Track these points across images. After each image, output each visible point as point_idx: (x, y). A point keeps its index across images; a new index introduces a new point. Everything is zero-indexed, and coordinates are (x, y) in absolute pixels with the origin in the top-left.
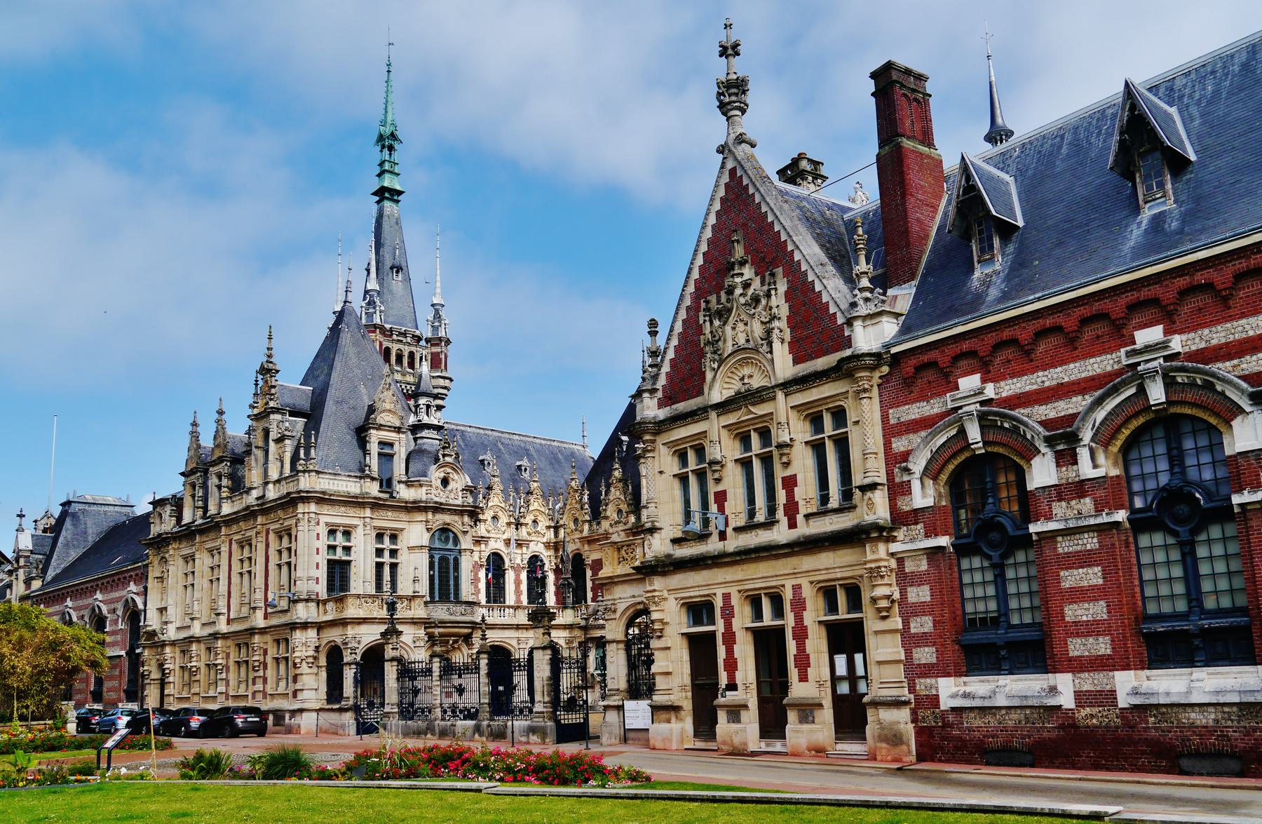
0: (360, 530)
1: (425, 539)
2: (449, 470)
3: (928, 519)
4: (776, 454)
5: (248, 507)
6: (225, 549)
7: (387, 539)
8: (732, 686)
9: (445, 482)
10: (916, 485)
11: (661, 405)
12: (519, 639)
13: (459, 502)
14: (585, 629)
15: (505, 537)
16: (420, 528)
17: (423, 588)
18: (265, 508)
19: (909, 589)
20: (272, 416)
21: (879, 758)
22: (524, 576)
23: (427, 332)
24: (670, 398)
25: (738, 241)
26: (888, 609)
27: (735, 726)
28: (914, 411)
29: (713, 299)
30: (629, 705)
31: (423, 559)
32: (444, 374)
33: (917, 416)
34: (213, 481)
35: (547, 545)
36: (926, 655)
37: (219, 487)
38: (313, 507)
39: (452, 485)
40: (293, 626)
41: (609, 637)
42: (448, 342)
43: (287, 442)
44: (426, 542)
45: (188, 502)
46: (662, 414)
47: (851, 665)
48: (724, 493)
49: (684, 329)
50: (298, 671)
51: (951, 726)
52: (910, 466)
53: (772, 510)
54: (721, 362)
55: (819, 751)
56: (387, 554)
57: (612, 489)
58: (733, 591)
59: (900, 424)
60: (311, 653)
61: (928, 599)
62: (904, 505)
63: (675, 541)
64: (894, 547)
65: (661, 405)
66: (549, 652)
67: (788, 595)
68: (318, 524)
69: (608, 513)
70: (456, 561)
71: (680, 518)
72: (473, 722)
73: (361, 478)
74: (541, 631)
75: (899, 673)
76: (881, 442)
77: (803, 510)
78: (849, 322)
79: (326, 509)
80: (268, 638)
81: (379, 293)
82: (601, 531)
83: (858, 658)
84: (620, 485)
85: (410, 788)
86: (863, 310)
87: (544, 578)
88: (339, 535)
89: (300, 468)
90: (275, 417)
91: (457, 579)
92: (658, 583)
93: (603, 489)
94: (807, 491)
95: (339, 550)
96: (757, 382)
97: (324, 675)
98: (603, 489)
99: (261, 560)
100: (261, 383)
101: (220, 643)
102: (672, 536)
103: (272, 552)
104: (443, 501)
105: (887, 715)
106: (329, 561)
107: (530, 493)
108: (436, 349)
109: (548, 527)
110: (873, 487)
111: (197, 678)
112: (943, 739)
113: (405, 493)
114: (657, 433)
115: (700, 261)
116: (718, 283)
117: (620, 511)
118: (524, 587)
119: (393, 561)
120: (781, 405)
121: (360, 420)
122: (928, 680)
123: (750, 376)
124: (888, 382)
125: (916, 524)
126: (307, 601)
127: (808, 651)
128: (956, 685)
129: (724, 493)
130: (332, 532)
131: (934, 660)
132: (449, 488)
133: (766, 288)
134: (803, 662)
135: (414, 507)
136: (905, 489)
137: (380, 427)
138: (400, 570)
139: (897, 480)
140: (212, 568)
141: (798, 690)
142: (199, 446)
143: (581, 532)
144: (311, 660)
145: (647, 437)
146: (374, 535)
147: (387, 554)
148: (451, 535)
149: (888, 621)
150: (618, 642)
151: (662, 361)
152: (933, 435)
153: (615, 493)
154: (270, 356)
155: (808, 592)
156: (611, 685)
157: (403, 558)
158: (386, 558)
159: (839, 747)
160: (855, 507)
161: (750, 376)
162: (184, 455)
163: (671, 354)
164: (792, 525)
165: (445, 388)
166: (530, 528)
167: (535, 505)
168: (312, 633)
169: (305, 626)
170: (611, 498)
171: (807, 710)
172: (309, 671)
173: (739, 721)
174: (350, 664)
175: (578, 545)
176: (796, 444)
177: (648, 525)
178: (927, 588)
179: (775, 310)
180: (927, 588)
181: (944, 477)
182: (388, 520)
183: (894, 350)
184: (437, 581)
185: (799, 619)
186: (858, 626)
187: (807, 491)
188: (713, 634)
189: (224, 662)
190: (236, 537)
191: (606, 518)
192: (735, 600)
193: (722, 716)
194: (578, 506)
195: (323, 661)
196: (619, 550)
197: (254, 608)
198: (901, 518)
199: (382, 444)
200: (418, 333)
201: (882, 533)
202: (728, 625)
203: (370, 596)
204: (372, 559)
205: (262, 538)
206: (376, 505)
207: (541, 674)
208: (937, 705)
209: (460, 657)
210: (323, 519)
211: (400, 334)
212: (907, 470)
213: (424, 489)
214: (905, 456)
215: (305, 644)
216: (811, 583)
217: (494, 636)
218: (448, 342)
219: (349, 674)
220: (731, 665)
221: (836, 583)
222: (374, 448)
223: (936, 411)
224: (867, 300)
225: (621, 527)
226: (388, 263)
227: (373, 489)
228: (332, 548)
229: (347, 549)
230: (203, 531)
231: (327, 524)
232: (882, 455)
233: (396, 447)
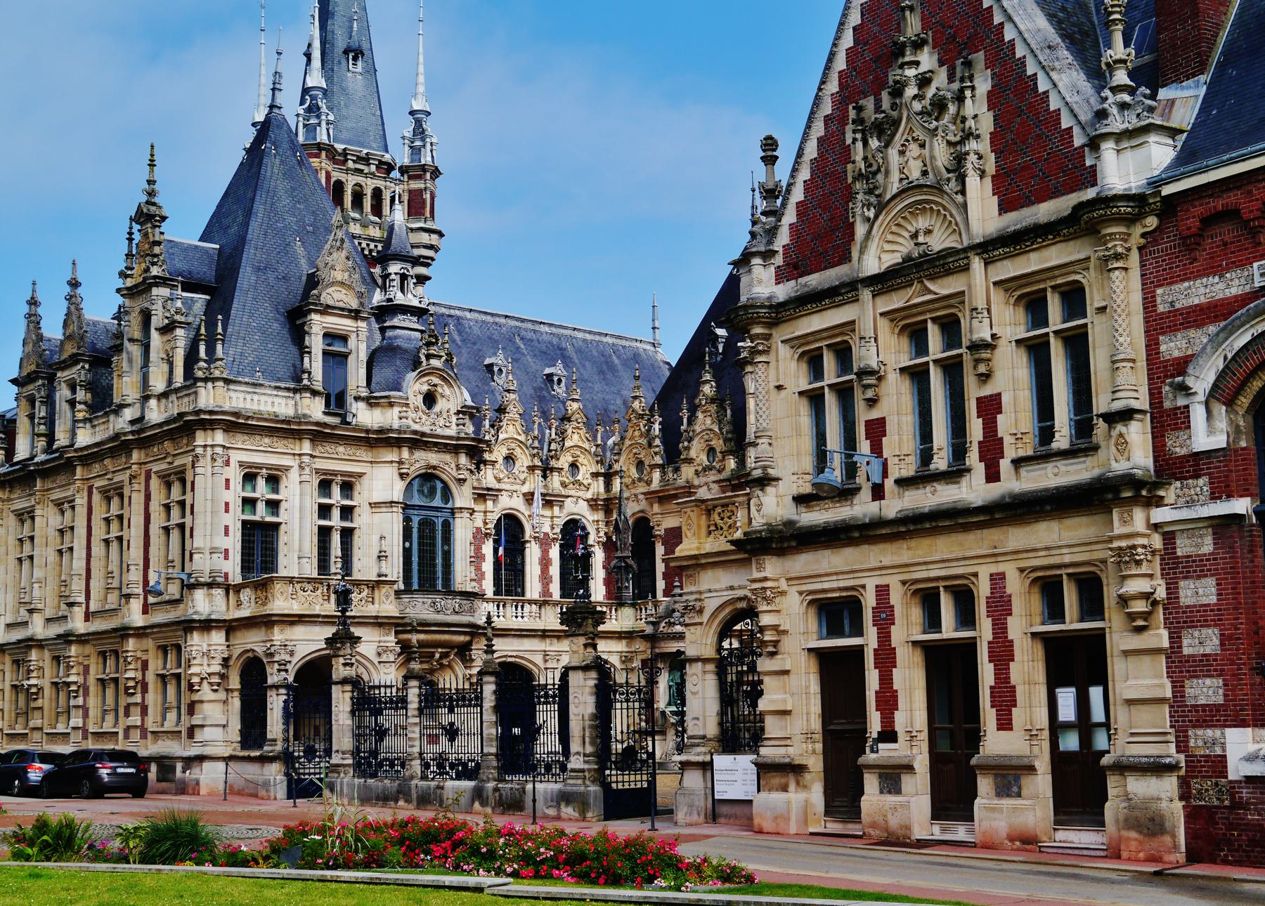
0: (294, 475)
1: (397, 490)
2: (436, 380)
3: (1219, 471)
4: (967, 359)
5: (117, 436)
6: (81, 501)
7: (336, 490)
8: (888, 735)
9: (430, 399)
10: (1198, 414)
11: (781, 277)
12: (545, 654)
13: (452, 432)
14: (653, 639)
15: (525, 489)
16: (390, 473)
17: (394, 569)
18: (145, 437)
19: (1182, 583)
20: (155, 291)
21: (1125, 854)
22: (555, 552)
23: (402, 157)
24: (796, 267)
25: (911, 9)
26: (1146, 616)
27: (891, 799)
28: (1198, 292)
29: (869, 103)
30: (721, 761)
31: (393, 523)
32: (429, 225)
33: (1203, 300)
34: (63, 393)
35: (593, 504)
36: (1206, 691)
37: (72, 403)
38: (219, 437)
39: (441, 405)
40: (189, 626)
41: (691, 652)
42: (436, 173)
43: (180, 332)
44: (398, 495)
45: (23, 426)
46: (782, 292)
47: (1083, 704)
48: (881, 422)
49: (820, 154)
50: (196, 697)
51: (1245, 806)
52: (1190, 382)
53: (959, 451)
54: (881, 207)
55: (1027, 841)
56: (336, 513)
57: (700, 415)
58: (894, 581)
59: (1174, 313)
60: (216, 668)
61: (1213, 599)
62: (1177, 447)
63: (802, 500)
64: (1160, 515)
65: (781, 277)
66: (594, 674)
67: (983, 589)
68: (227, 463)
69: (693, 454)
70: (447, 527)
71: (808, 463)
72: (472, 784)
73: (295, 391)
74: (582, 640)
75: (1161, 719)
76: (1141, 342)
77: (1010, 452)
78: (1094, 144)
79: (240, 440)
80: (149, 643)
81: (325, 92)
82: (681, 482)
83: (1096, 693)
84: (713, 408)
85: (371, 882)
86: (1117, 123)
87: (588, 555)
88: (261, 483)
89: (200, 374)
90: (161, 292)
91: (447, 556)
92: (772, 568)
93: (685, 414)
94: (1016, 420)
95: (261, 507)
96: (939, 241)
97: (236, 703)
98: (685, 414)
99: (137, 520)
100: (137, 237)
101: (74, 650)
102: (795, 492)
103: (155, 507)
104: (426, 429)
105: (1140, 787)
106: (245, 523)
107: (566, 419)
108: (416, 185)
109: (595, 475)
110: (1127, 415)
111: (39, 703)
112: (1231, 827)
113: (365, 417)
114: (774, 323)
115: (848, 40)
116: (876, 78)
117: (711, 451)
118: (555, 570)
119: (347, 524)
120: (979, 280)
121: (294, 301)
122: (1209, 732)
123: (928, 232)
124: (1155, 242)
125: (1197, 477)
126: (210, 586)
127: (1013, 682)
128: (1255, 741)
129: (881, 422)
130: (249, 478)
131: (1220, 700)
132: (437, 408)
133: (956, 86)
134: (1005, 698)
135: (380, 440)
136: (1180, 420)
137: (326, 310)
138: (358, 540)
139: (1167, 404)
140: (61, 532)
141: (996, 743)
142: (40, 338)
143: (649, 483)
144: (216, 679)
145: (757, 330)
146: (316, 483)
147: (336, 513)
148: (439, 485)
149: (1146, 635)
150: (705, 661)
151: (784, 205)
152: (1230, 331)
153: (704, 421)
154: (151, 194)
155: (1015, 585)
156: (692, 729)
157: (363, 520)
158: (335, 520)
159: (1060, 835)
160: (1096, 448)
161: (928, 232)
162: (17, 352)
163: (798, 195)
164: (993, 475)
165: (431, 247)
166: (568, 479)
167: (575, 438)
168: (218, 637)
169: (207, 625)
170: (698, 428)
171: (1010, 776)
172: (213, 696)
173: (898, 791)
174: (276, 687)
175: (643, 504)
176: (1002, 343)
177: (757, 473)
178: (1211, 582)
179: (970, 123)
180: (1211, 582)
181: (1244, 401)
182: (338, 460)
183: (1167, 190)
184: (415, 559)
185: (1000, 629)
186: (1098, 639)
187: (1016, 420)
188: (859, 651)
189: (80, 680)
190: (99, 483)
191: (689, 461)
192: (897, 597)
193: (871, 783)
194: (644, 441)
195: (235, 682)
196: (709, 512)
197: (128, 596)
198: (1172, 467)
199: (330, 336)
200: (387, 158)
201: (1141, 491)
202: (884, 637)
203: (310, 580)
204: (313, 522)
205: (139, 485)
206: (319, 435)
207: (581, 710)
208: (1223, 772)
209: (452, 679)
210: (236, 457)
211: (359, 159)
212: (1184, 389)
213: (396, 410)
214: (1182, 365)
215: (207, 654)
216: (1022, 570)
217: (505, 648)
218: (436, 173)
219: (276, 704)
220: (888, 701)
221: (1063, 571)
222: (316, 343)
223: (1234, 291)
224: (1123, 106)
225: (713, 476)
226: (341, 43)
227: (315, 409)
228: (249, 503)
229: (274, 505)
230: (46, 472)
231: (241, 464)
232: (1142, 364)
233: (352, 343)
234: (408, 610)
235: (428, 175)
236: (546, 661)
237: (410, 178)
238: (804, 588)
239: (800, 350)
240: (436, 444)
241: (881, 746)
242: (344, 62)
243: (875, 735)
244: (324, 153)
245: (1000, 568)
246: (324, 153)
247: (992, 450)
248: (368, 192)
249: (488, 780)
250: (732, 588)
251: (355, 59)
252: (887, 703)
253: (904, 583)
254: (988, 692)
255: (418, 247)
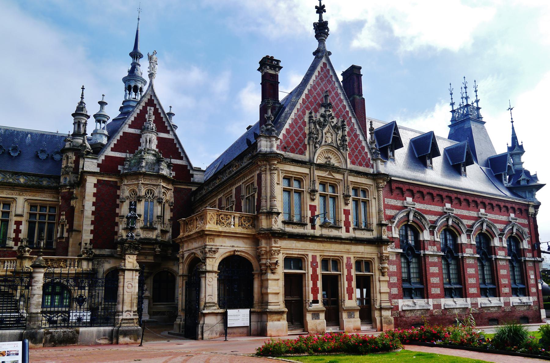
8: (316, 301)
27: (318, 321)
36: (395, 291)
48: (315, 207)
61: (396, 270)
83: (365, 290)
134: (350, 292)
150: (215, 272)
173: (319, 319)
238: (285, 252)
239: (285, 175)
241: (313, 305)
243: (311, 301)
245: (349, 256)
247: (347, 224)
249: (40, 328)
250: (233, 246)
252: (315, 291)
253: (320, 256)
254: (346, 289)
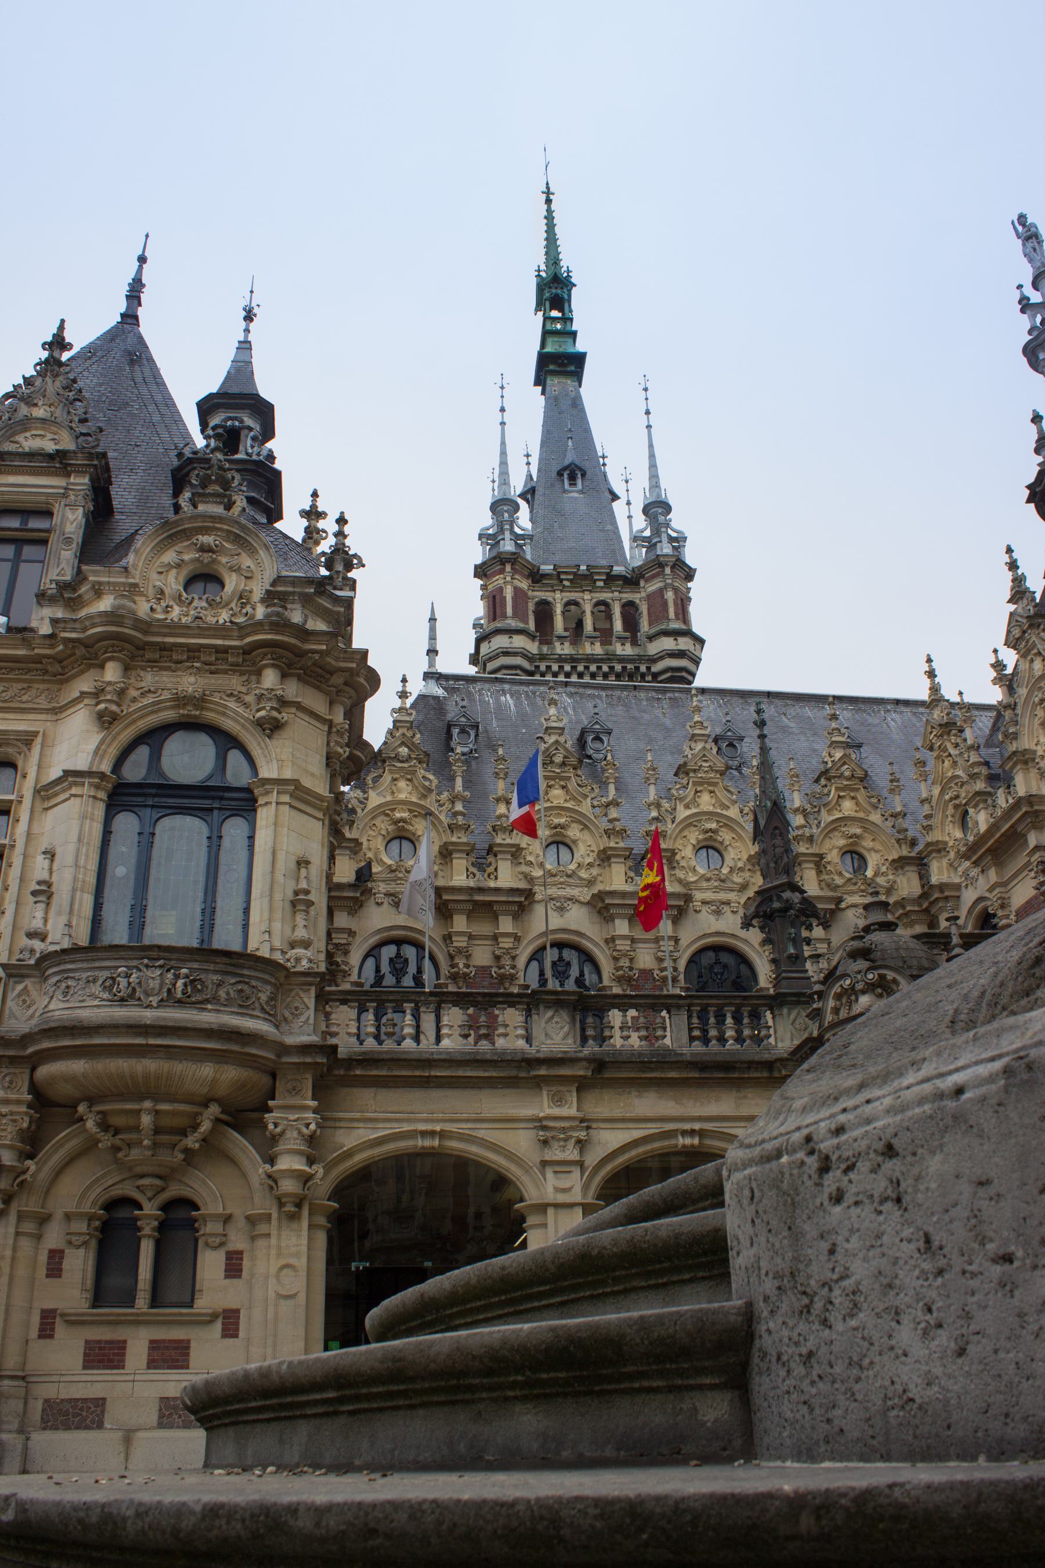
108: (653, 586)
165: (681, 654)
234: (51, 1007)
235: (668, 570)
236: (545, 1142)
237: (647, 581)
240: (194, 652)
242: (558, 485)
244: (508, 568)
246: (508, 568)
248: (588, 608)
251: (572, 478)
255: (661, 658)
